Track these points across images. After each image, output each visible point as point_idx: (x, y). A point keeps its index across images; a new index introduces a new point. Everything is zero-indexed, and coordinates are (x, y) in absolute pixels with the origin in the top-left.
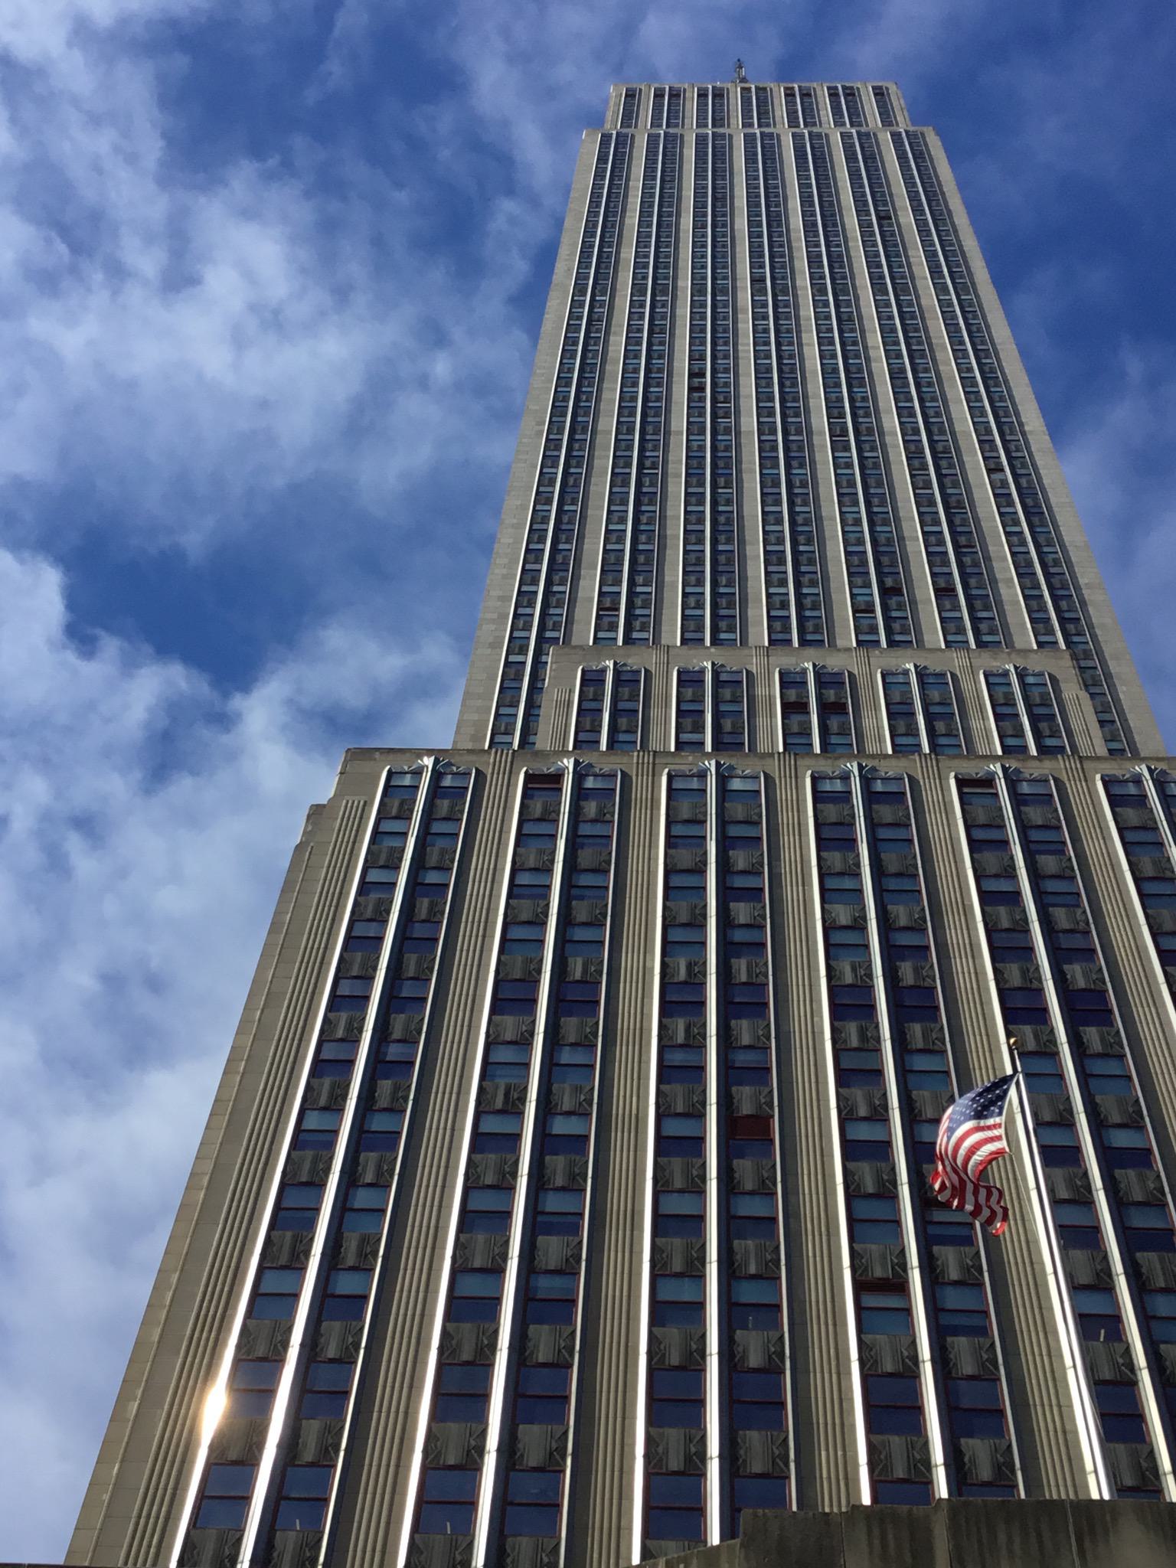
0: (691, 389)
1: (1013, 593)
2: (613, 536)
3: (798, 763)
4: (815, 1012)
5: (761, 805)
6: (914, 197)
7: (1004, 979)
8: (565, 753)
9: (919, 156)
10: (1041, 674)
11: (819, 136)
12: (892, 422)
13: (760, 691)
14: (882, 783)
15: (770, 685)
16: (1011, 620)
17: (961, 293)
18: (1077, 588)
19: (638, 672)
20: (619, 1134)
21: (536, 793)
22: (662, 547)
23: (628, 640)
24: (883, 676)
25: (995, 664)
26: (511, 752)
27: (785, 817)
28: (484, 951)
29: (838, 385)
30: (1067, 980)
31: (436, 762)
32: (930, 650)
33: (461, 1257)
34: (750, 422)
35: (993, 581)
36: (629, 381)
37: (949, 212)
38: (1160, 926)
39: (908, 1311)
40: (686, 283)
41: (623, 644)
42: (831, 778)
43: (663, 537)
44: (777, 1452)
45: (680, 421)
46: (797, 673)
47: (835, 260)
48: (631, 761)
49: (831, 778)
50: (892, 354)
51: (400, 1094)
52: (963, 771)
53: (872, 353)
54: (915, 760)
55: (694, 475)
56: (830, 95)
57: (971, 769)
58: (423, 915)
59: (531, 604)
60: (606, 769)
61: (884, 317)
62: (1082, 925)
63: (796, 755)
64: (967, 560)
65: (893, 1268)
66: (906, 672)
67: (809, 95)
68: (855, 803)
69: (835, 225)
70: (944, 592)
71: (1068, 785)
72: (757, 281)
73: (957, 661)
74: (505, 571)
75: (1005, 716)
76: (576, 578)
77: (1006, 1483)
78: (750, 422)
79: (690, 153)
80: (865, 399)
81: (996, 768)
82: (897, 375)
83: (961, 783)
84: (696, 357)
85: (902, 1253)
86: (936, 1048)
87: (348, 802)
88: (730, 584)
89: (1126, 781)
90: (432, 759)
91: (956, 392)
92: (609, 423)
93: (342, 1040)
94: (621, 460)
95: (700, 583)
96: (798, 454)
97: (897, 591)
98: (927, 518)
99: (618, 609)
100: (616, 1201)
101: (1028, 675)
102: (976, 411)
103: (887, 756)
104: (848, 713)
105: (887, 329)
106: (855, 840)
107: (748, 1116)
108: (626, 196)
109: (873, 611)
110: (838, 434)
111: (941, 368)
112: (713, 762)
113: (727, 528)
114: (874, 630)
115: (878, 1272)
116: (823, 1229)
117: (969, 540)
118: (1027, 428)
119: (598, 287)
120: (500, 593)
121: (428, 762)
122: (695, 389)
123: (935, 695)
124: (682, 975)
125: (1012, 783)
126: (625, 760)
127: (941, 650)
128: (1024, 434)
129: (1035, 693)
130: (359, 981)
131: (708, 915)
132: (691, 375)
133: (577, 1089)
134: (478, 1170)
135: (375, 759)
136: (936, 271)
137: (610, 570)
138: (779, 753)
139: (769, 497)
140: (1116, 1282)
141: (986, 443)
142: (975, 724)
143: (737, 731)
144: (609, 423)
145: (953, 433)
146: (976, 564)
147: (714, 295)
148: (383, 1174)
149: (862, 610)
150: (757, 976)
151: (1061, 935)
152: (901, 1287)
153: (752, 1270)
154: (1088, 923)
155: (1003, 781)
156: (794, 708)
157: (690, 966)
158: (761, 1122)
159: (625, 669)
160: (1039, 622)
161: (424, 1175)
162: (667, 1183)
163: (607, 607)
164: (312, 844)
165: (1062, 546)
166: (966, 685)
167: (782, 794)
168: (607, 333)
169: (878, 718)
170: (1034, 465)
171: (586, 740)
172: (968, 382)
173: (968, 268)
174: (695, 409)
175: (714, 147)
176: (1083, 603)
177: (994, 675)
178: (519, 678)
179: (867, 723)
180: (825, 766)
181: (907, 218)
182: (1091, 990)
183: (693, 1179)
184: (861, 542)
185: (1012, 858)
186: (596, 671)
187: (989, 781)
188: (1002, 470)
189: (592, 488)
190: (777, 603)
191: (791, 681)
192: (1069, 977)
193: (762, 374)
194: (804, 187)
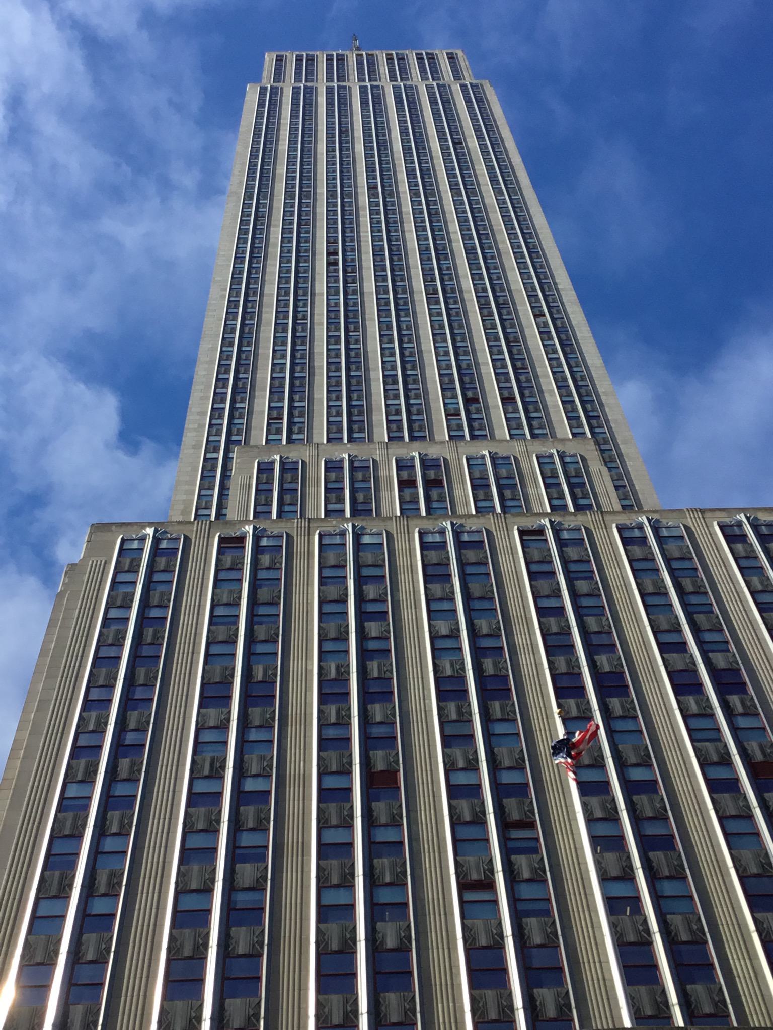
1: (554, 399)
2: (277, 367)
4: (426, 697)
5: (384, 554)
6: (477, 130)
7: (554, 667)
8: (247, 522)
9: (479, 101)
10: (575, 455)
11: (411, 87)
12: (468, 284)
13: (382, 473)
14: (468, 536)
15: (390, 469)
16: (554, 418)
17: (512, 194)
18: (598, 396)
19: (298, 462)
20: (292, 789)
21: (227, 550)
22: (312, 374)
23: (290, 440)
24: (467, 459)
25: (543, 449)
27: (401, 561)
28: (178, 778)
29: (430, 259)
30: (597, 666)
31: (156, 531)
32: (499, 440)
33: (182, 882)
34: (370, 285)
35: (541, 392)
36: (285, 258)
37: (501, 138)
39: (495, 902)
40: (322, 190)
41: (287, 443)
42: (432, 533)
43: (312, 367)
44: (407, 1007)
45: (321, 286)
48: (293, 526)
49: (432, 533)
50: (466, 237)
52: (523, 524)
53: (452, 236)
55: (332, 323)
56: (418, 59)
57: (529, 523)
58: (141, 681)
59: (221, 417)
60: (276, 532)
61: (460, 212)
62: (606, 628)
63: (407, 517)
64: (523, 378)
65: (484, 872)
66: (483, 457)
67: (403, 59)
69: (424, 149)
70: (508, 400)
71: (594, 532)
72: (372, 188)
73: (517, 448)
74: (202, 395)
75: (551, 485)
77: (566, 1018)
78: (370, 285)
79: (322, 100)
80: (449, 268)
81: (546, 522)
82: (470, 252)
83: (522, 533)
84: (331, 241)
85: (491, 861)
86: (510, 717)
87: (93, 561)
88: (360, 399)
89: (633, 528)
90: (153, 529)
91: (511, 262)
92: (272, 289)
93: (93, 732)
94: (281, 314)
95: (339, 398)
96: (404, 307)
97: (476, 400)
98: (494, 349)
99: (282, 419)
100: (291, 836)
102: (525, 275)
103: (472, 516)
104: (443, 487)
105: (462, 220)
106: (450, 576)
107: (382, 771)
108: (278, 130)
109: (459, 415)
111: (500, 246)
112: (350, 525)
113: (356, 360)
114: (460, 427)
115: (475, 876)
116: (436, 848)
117: (523, 364)
118: (559, 286)
119: (262, 194)
120: (199, 410)
121: (150, 531)
122: (332, 264)
123: (503, 472)
124: (333, 674)
125: (557, 532)
126: (289, 525)
127: (507, 441)
128: (557, 290)
129: (571, 468)
130: (104, 689)
131: (352, 715)
132: (328, 254)
133: (262, 758)
134: (193, 819)
135: (112, 531)
136: (493, 180)
137: (276, 391)
138: (396, 516)
139: (385, 337)
140: (637, 874)
141: (532, 297)
142: (531, 491)
143: (367, 502)
144: (272, 289)
145: (510, 291)
146: (529, 380)
147: (342, 198)
149: (452, 414)
150: (385, 673)
152: (491, 886)
153: (388, 879)
154: (610, 627)
155: (550, 530)
156: (406, 484)
157: (338, 668)
158: (390, 776)
159: (287, 461)
160: (573, 419)
161: (153, 825)
162: (326, 821)
163: (274, 418)
165: (587, 367)
166: (524, 465)
167: (398, 545)
169: (465, 489)
170: (565, 311)
171: (261, 512)
172: (518, 255)
173: (515, 176)
174: (332, 277)
175: (339, 96)
176: (601, 405)
178: (214, 469)
179: (457, 493)
180: (428, 525)
181: (473, 143)
182: (614, 673)
183: (344, 818)
184: (449, 367)
185: (558, 584)
187: (541, 531)
188: (544, 315)
189: (261, 335)
190: (392, 411)
191: (403, 465)
192: (598, 664)
193: (378, 253)
194: (402, 122)
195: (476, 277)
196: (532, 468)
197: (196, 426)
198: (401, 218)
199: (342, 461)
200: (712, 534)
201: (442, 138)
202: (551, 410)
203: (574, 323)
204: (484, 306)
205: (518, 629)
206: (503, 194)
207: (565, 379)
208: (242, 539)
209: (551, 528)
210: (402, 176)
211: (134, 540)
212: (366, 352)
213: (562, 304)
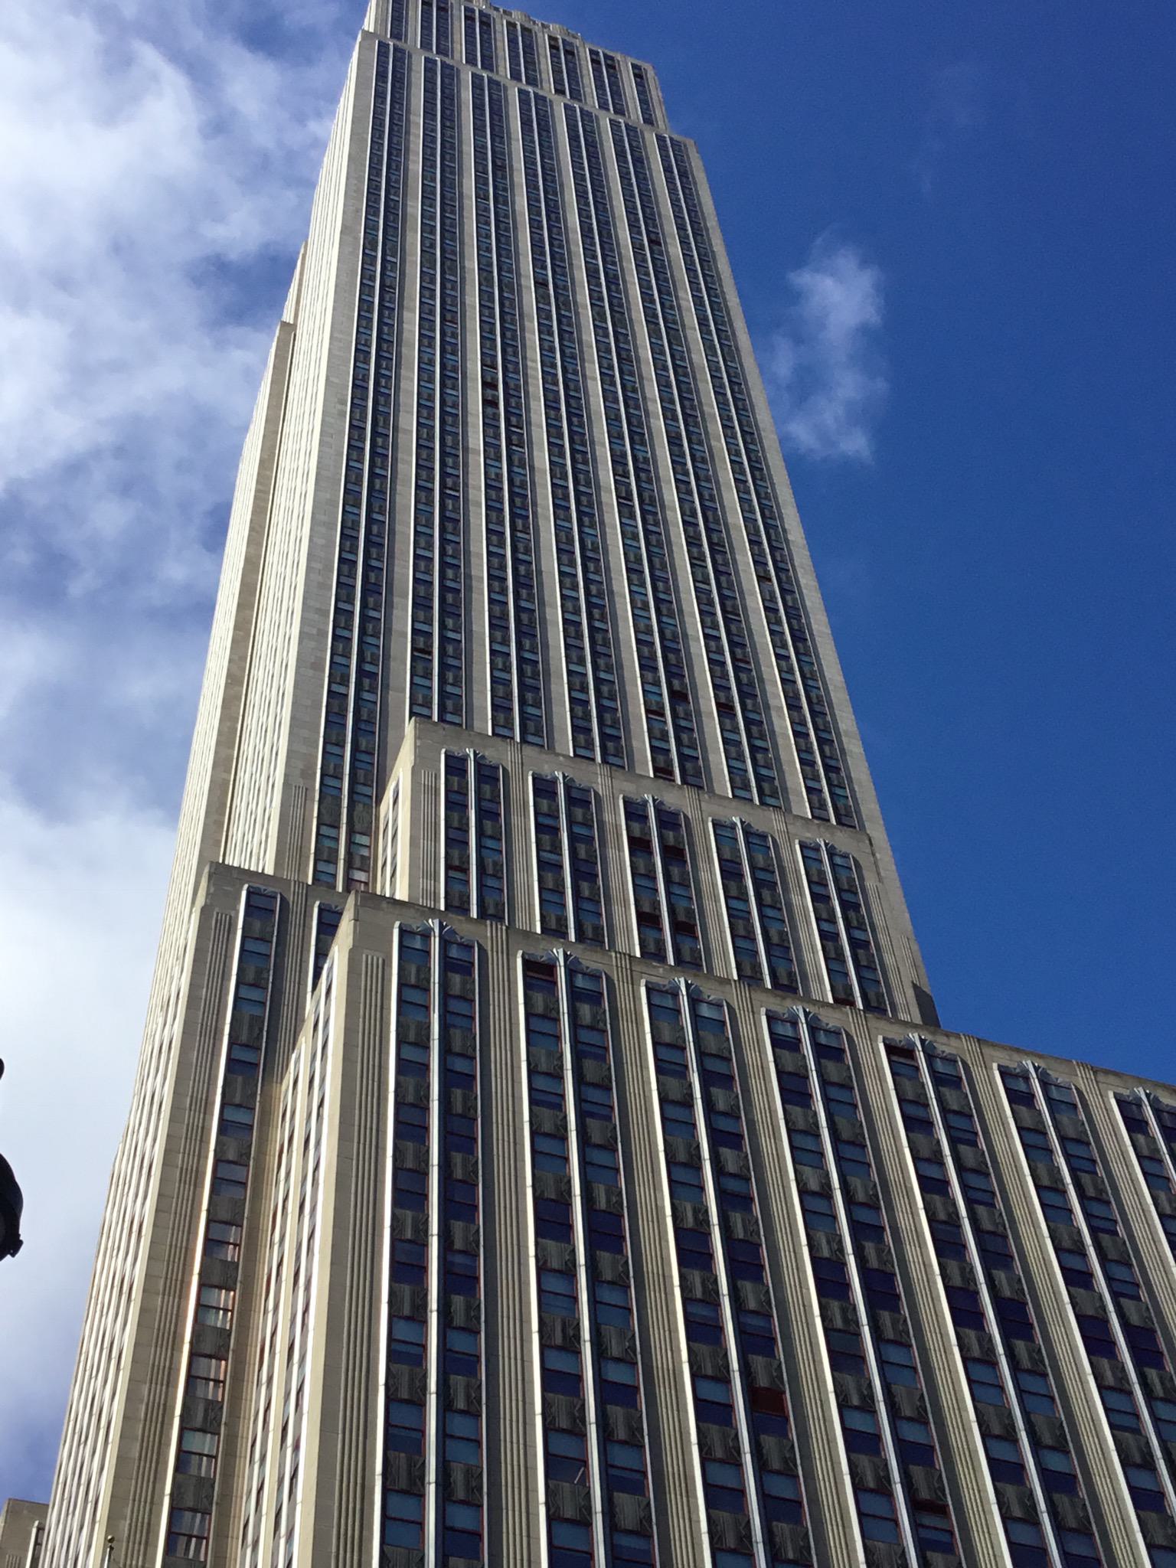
0: (485, 402)
1: (783, 724)
3: (752, 996)
5: (728, 1039)
6: (681, 228)
7: (947, 1275)
9: (683, 175)
10: (845, 856)
12: (671, 495)
13: (607, 817)
14: (826, 1035)
17: (727, 358)
18: (838, 735)
20: (662, 1389)
22: (469, 588)
25: (808, 835)
26: (504, 928)
27: (751, 1057)
30: (996, 1286)
33: (553, 1505)
34: (542, 458)
35: (767, 707)
38: (1060, 1242)
42: (783, 1021)
43: (468, 577)
45: (477, 440)
46: (638, 804)
47: (613, 281)
49: (783, 1021)
50: (669, 415)
51: (472, 1314)
53: (651, 408)
54: (848, 1014)
55: (493, 508)
57: (897, 1034)
60: (593, 966)
62: (1001, 1228)
63: (749, 985)
66: (733, 826)
67: (573, 54)
68: (806, 1053)
70: (725, 709)
72: (540, 284)
74: (320, 578)
76: (390, 605)
78: (542, 458)
79: (467, 96)
80: (646, 460)
82: (674, 441)
84: (488, 364)
86: (903, 1340)
91: (727, 475)
93: (409, 1241)
95: (506, 642)
98: (706, 613)
101: (836, 855)
110: (624, 498)
118: (790, 537)
120: (318, 606)
122: (489, 403)
128: (787, 541)
129: (843, 875)
132: (485, 384)
136: (703, 322)
137: (421, 604)
138: (735, 981)
141: (755, 542)
142: (795, 899)
148: (472, 1402)
151: (986, 1236)
153: (791, 1555)
154: (1005, 1228)
156: (639, 846)
164: (217, 910)
165: (825, 683)
166: (785, 854)
167: (745, 1031)
168: (401, 306)
176: (843, 751)
177: (810, 848)
181: (675, 250)
186: (456, 757)
188: (770, 580)
194: (579, 178)
195: (682, 484)
196: (795, 862)
197: (314, 631)
198: (581, 351)
199: (554, 781)
200: (1108, 1110)
201: (633, 226)
202: (780, 741)
203: (808, 603)
204: (693, 542)
205: (899, 1203)
206: (716, 355)
207: (797, 697)
208: (550, 968)
209: (923, 1051)
210: (582, 275)
211: (417, 933)
212: (539, 572)
213: (794, 570)
